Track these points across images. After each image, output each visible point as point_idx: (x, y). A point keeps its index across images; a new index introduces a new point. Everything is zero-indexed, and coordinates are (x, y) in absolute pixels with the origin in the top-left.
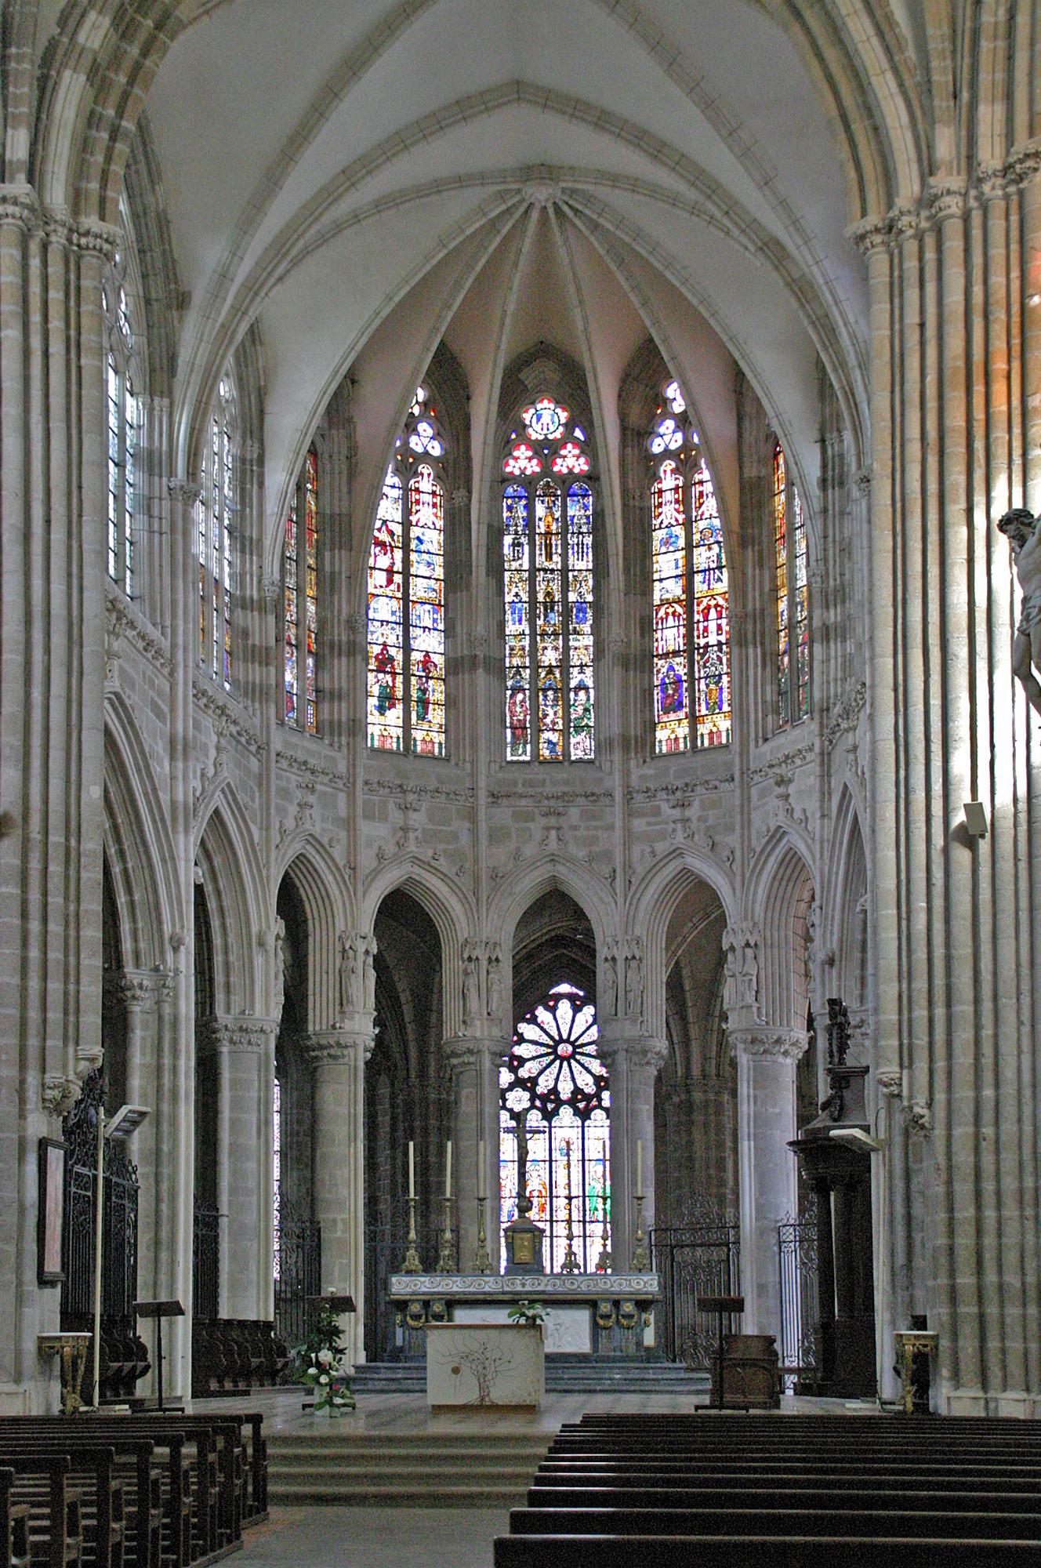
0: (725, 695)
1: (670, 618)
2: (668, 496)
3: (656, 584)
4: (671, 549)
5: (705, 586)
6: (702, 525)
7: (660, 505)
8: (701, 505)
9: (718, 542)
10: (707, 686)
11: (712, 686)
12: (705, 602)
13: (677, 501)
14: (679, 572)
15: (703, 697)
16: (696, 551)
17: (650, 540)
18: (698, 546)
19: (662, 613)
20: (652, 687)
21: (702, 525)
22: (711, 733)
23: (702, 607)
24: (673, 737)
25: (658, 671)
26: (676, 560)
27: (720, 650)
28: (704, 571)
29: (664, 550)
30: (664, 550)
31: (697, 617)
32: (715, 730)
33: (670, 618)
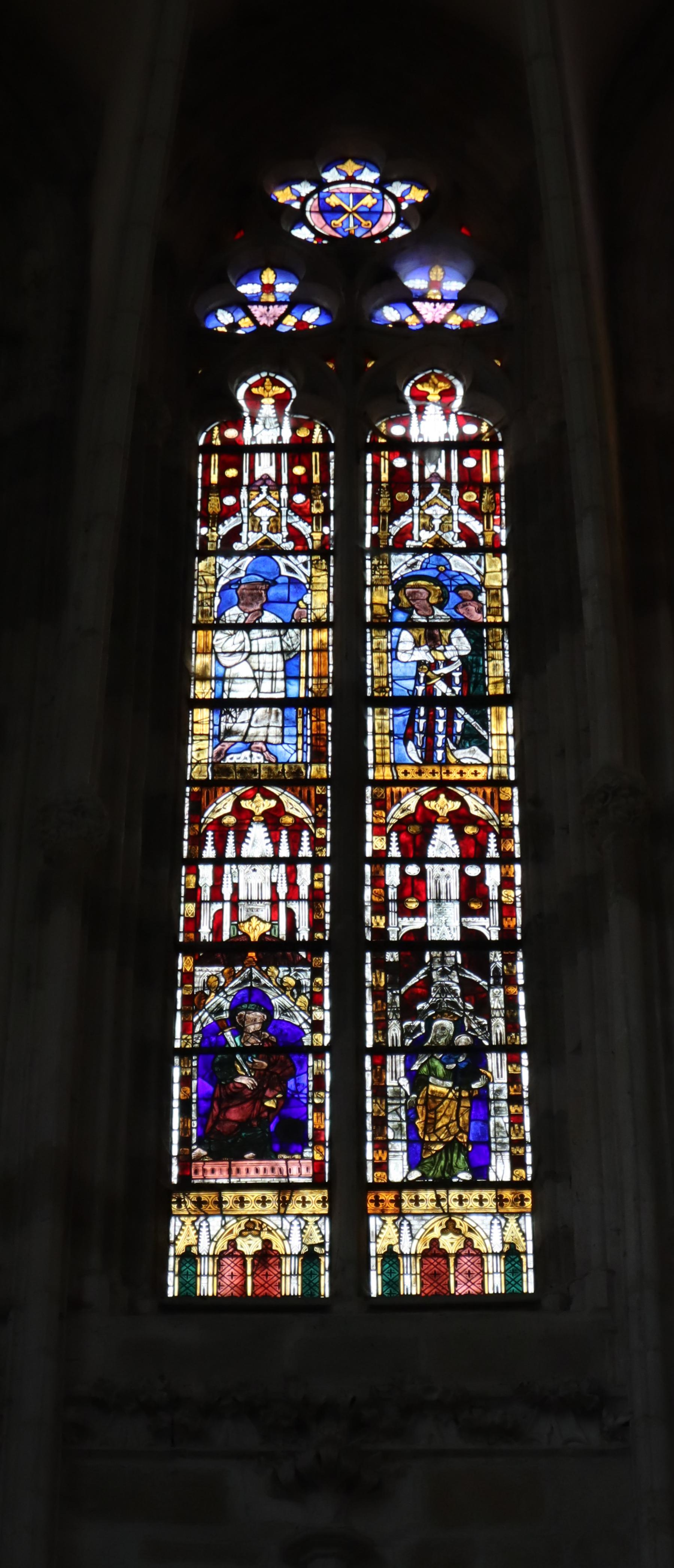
0: (500, 1121)
1: (258, 834)
2: (265, 465)
3: (201, 715)
4: (268, 617)
5: (413, 753)
6: (400, 564)
7: (232, 487)
8: (398, 510)
9: (472, 629)
10: (417, 1081)
11: (439, 1087)
12: (411, 802)
13: (297, 485)
14: (297, 690)
15: (396, 1118)
16: (375, 640)
17: (188, 578)
18: (384, 624)
19: (224, 804)
20: (167, 1054)
21: (400, 564)
22: (434, 1252)
23: (396, 814)
24: (250, 1246)
25: (194, 1003)
26: (290, 656)
27: (479, 963)
28: (410, 702)
29: (233, 614)
30: (233, 614)
31: (373, 843)
32: (450, 1243)
33: (258, 834)
